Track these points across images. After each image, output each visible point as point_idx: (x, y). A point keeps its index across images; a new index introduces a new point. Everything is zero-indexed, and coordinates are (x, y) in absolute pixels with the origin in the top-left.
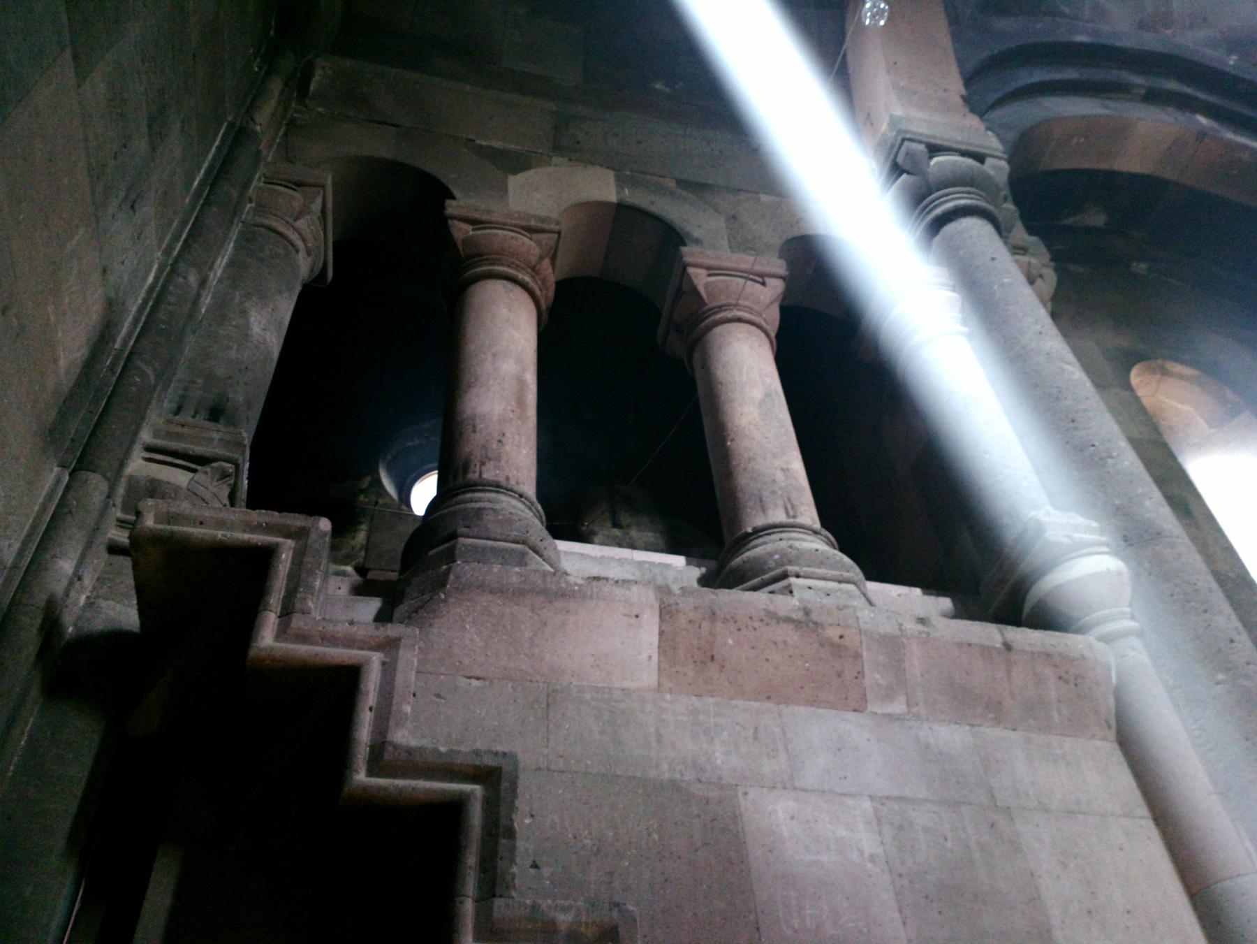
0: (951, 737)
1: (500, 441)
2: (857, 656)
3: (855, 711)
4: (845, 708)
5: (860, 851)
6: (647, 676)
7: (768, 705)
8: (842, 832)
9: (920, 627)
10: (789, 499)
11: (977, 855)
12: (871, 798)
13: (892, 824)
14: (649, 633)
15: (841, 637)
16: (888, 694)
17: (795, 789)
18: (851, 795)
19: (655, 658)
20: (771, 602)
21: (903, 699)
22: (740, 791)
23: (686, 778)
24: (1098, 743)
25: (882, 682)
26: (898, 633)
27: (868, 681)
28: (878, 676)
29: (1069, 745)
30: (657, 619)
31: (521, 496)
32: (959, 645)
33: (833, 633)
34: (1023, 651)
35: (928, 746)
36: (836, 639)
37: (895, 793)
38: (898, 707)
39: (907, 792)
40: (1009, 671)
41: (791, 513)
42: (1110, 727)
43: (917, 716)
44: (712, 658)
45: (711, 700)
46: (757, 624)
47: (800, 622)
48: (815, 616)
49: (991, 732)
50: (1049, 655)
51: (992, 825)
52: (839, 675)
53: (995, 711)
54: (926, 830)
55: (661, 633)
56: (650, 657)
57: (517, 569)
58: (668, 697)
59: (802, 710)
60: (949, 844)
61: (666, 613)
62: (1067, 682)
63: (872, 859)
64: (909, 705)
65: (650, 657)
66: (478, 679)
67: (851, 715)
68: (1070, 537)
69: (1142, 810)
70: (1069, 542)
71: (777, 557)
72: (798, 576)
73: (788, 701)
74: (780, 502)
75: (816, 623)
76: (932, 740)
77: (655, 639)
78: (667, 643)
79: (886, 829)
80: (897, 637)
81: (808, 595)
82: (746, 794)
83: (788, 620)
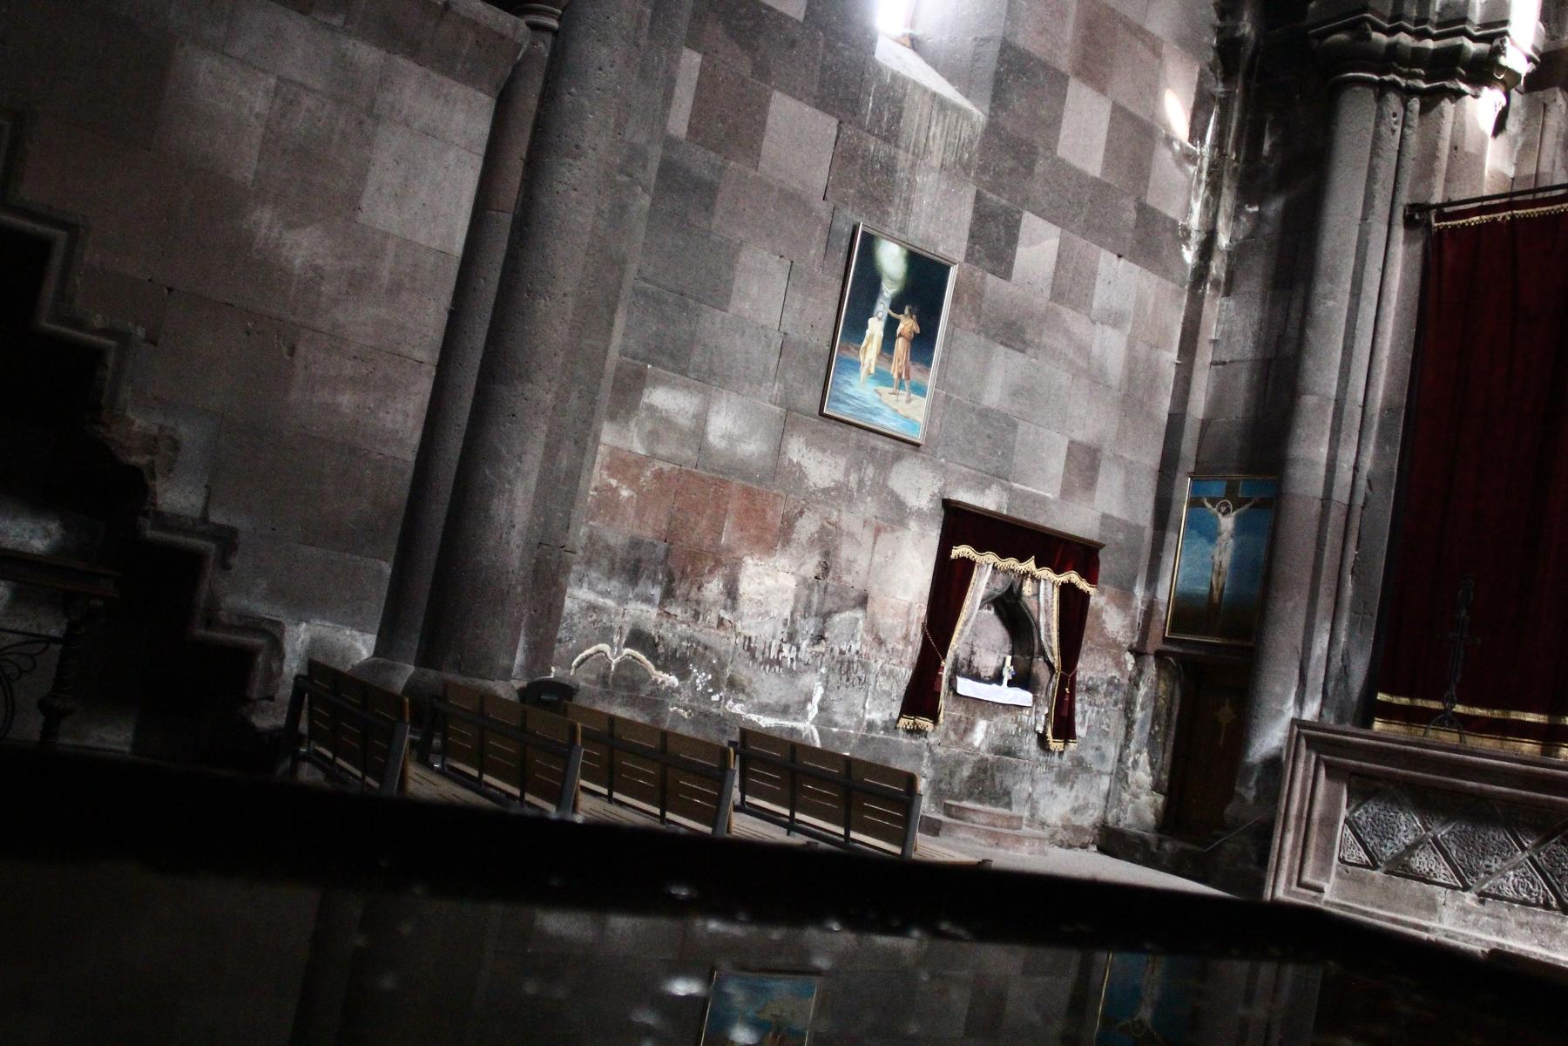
5: (251, 109)
8: (244, 93)
11: (336, 138)
13: (284, 99)
18: (265, 71)
21: (343, 17)
24: (481, 95)
38: (337, 21)
39: (310, 82)
40: (437, 25)
49: (400, 60)
50: (476, 23)
51: (361, 123)
53: (414, 51)
54: (308, 110)
60: (320, 125)
63: (257, 116)
67: (294, 14)
69: (482, 150)
79: (278, 101)
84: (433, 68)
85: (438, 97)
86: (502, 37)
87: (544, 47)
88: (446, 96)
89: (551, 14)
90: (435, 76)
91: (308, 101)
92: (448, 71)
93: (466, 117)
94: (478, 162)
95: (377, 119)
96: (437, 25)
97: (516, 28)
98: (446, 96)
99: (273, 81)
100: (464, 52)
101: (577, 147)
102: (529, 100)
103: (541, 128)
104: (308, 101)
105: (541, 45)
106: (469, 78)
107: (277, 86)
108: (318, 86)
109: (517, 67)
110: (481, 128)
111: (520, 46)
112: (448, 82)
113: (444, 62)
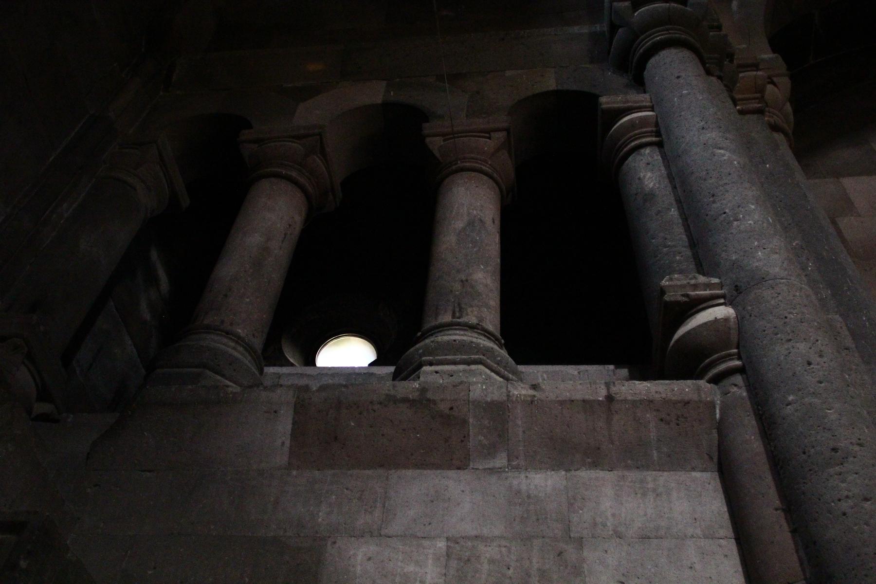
0: (544, 482)
1: (226, 296)
2: (465, 422)
3: (459, 468)
4: (449, 467)
6: (281, 459)
7: (380, 471)
8: (411, 568)
9: (531, 392)
10: (459, 304)
12: (448, 539)
13: (460, 559)
14: (284, 425)
15: (451, 408)
16: (490, 451)
17: (381, 535)
19: (288, 443)
20: (394, 386)
22: (329, 543)
23: (288, 534)
24: (696, 474)
25: (485, 442)
26: (505, 398)
27: (471, 444)
28: (481, 438)
29: (664, 477)
30: (291, 412)
31: (227, 333)
32: (562, 403)
33: (443, 407)
34: (625, 401)
35: (519, 492)
36: (447, 411)
37: (474, 533)
38: (500, 461)
39: (485, 531)
40: (609, 421)
41: (457, 314)
42: (711, 458)
43: (517, 468)
44: (336, 438)
45: (331, 472)
46: (376, 407)
47: (414, 400)
48: (429, 395)
49: (584, 474)
51: (560, 554)
52: (446, 441)
53: (595, 458)
54: (491, 561)
55: (294, 423)
56: (283, 443)
57: (190, 387)
58: (294, 473)
59: (409, 473)
60: (511, 572)
61: (301, 407)
62: (668, 423)
64: (509, 461)
65: (283, 443)
66: (150, 471)
67: (452, 473)
68: (687, 296)
69: (726, 530)
70: (685, 299)
71: (421, 351)
72: (431, 364)
73: (397, 466)
74: (451, 308)
75: (429, 400)
76: (524, 487)
77: (289, 427)
78: (298, 432)
79: (454, 564)
80: (502, 403)
81: (431, 378)
82: (335, 543)
83: (405, 400)
84: (628, 467)
85: (644, 495)
86: (687, 403)
87: (737, 388)
88: (654, 490)
89: (729, 357)
90: (633, 475)
91: (488, 552)
92: (645, 465)
93: (692, 501)
94: (731, 547)
95: (580, 542)
96: (609, 421)
97: (699, 389)
98: (654, 490)
99: (441, 544)
100: (653, 435)
101: (835, 450)
102: (748, 440)
103: (778, 463)
104: (488, 552)
105: (734, 389)
106: (674, 462)
107: (448, 547)
108: (497, 532)
109: (721, 427)
110: (715, 506)
111: (712, 405)
112: (650, 475)
113: (633, 456)
